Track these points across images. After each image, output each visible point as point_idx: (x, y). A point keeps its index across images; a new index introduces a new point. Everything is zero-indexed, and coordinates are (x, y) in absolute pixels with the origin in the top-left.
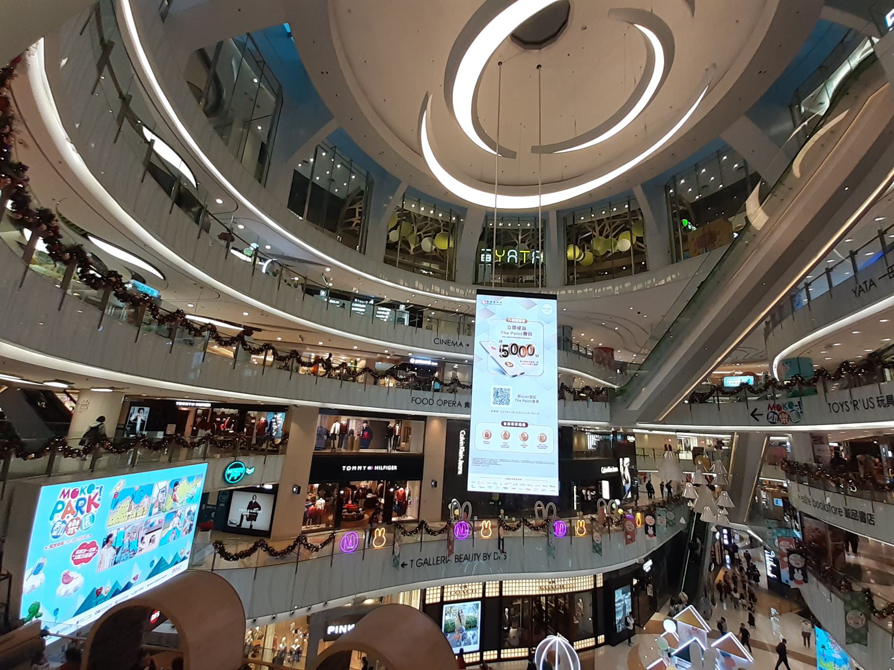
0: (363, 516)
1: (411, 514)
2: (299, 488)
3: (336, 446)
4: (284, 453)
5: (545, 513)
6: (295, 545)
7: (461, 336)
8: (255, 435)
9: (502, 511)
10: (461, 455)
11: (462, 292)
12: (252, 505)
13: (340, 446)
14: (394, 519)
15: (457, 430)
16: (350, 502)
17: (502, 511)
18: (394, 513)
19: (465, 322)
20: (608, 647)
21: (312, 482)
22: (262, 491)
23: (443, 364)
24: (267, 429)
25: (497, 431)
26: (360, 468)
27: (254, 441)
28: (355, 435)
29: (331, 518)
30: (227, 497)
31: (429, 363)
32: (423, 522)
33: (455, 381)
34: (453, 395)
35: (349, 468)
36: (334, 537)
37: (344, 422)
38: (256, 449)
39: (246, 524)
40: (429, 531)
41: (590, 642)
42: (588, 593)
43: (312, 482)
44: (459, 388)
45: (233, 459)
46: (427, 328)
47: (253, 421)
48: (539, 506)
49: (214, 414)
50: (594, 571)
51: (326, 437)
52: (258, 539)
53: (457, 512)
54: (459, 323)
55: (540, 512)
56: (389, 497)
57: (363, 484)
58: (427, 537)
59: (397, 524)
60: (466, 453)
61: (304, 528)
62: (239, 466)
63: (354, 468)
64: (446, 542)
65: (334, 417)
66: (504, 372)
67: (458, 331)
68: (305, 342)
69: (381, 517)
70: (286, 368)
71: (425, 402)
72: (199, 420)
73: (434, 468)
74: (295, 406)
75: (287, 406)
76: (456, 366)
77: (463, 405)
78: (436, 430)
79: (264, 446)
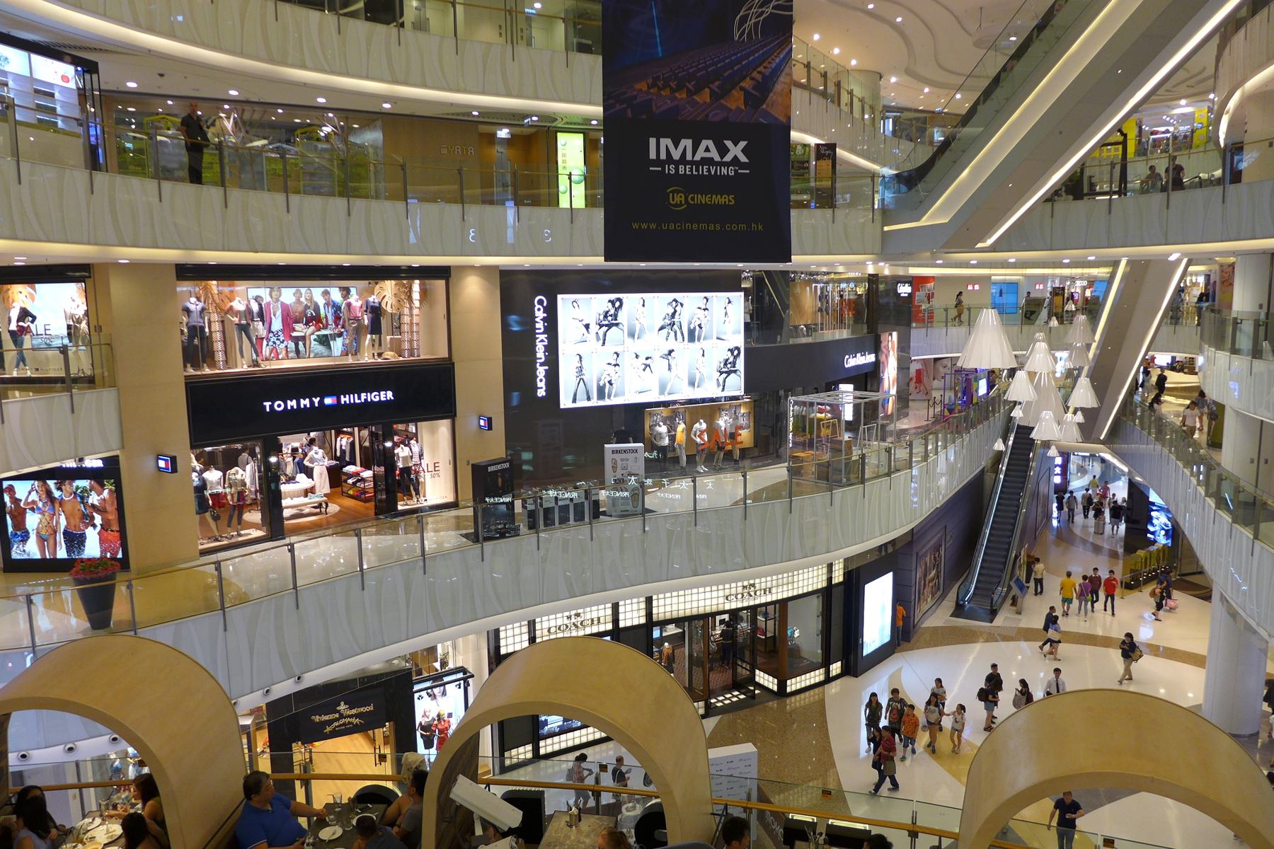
10: (540, 354)
20: (848, 681)
26: (305, 402)
35: (279, 406)
41: (817, 676)
42: (814, 597)
50: (828, 557)
63: (292, 404)
73: (480, 385)
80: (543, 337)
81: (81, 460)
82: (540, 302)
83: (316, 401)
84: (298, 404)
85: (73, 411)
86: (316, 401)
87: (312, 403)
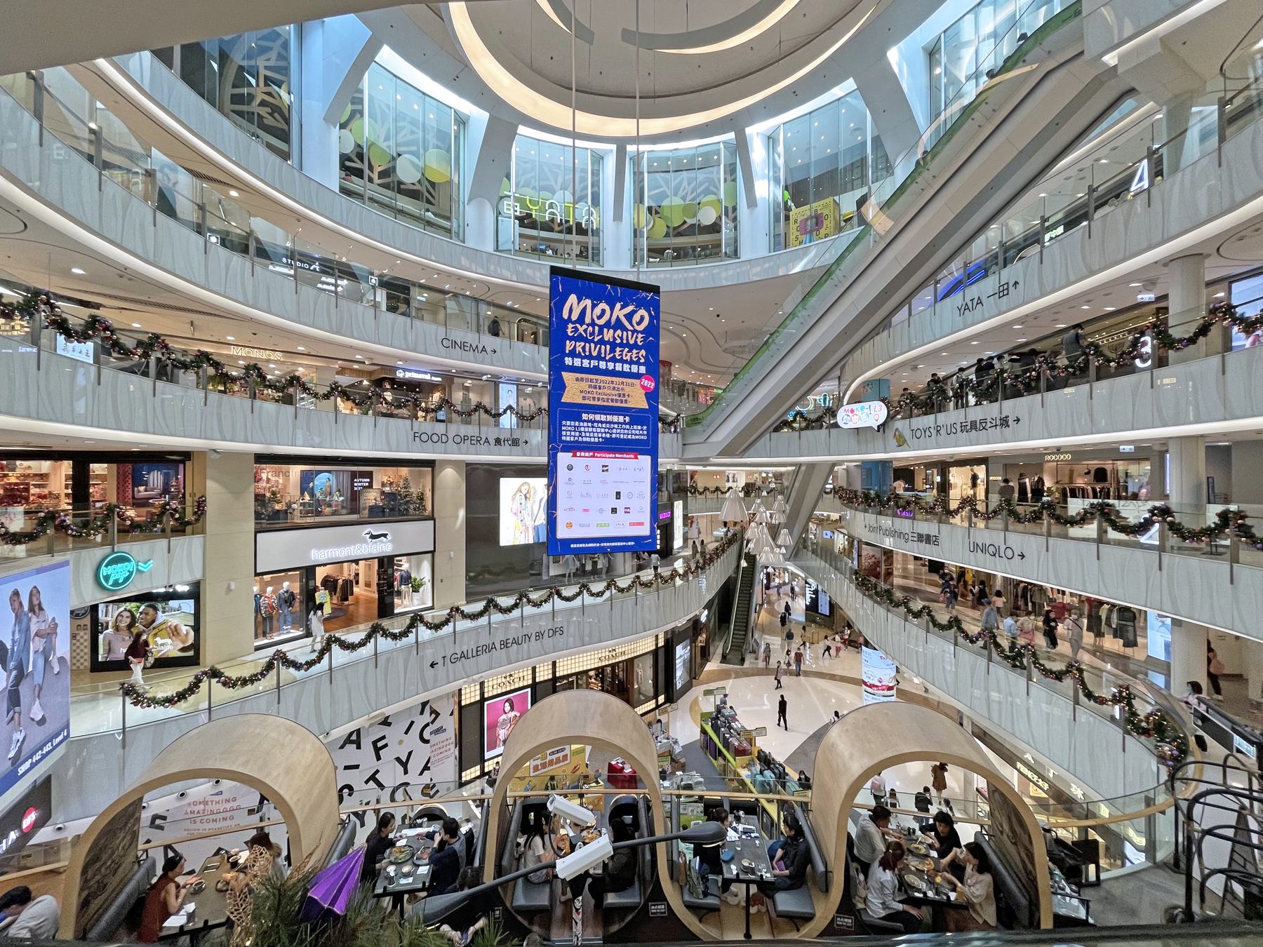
41: (652, 705)
50: (654, 632)
71: (435, 438)
77: (492, 442)
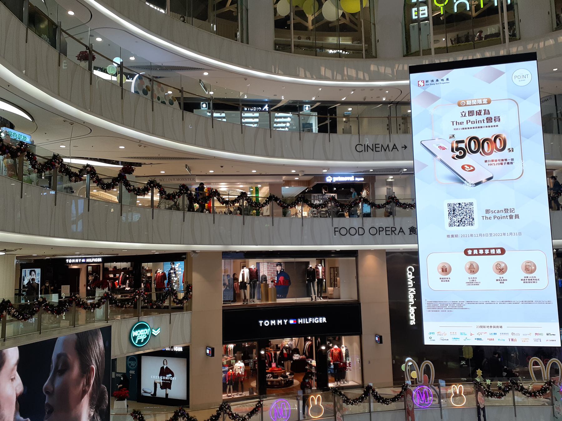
0: (291, 383)
1: (352, 378)
2: (213, 350)
3: (248, 297)
4: (189, 309)
5: (546, 374)
6: (219, 414)
7: (394, 136)
8: (153, 290)
9: (479, 372)
10: (411, 299)
11: (389, 71)
12: (164, 372)
13: (252, 296)
14: (331, 385)
15: (401, 268)
16: (274, 365)
17: (479, 372)
18: (330, 378)
19: (396, 115)
21: (226, 341)
22: (172, 354)
23: (371, 179)
24: (166, 282)
25: (459, 263)
26: (280, 322)
27: (154, 298)
28: (269, 282)
29: (254, 384)
30: (136, 363)
31: (352, 179)
32: (369, 388)
33: (392, 200)
34: (390, 219)
35: (267, 323)
36: (262, 405)
37: (253, 267)
38: (159, 307)
39: (161, 393)
40: (379, 399)
43: (226, 341)
44: (397, 209)
45: (135, 320)
46: (344, 132)
47: (149, 275)
48: (536, 363)
49: (106, 270)
51: (235, 288)
52: (177, 408)
53: (414, 374)
54: (389, 118)
55: (538, 374)
56: (322, 357)
57: (287, 342)
58: (375, 406)
59: (336, 391)
60: (418, 296)
61: (225, 396)
62: (142, 327)
63: (273, 322)
64: (403, 413)
65: (239, 261)
66: (461, 180)
67: (389, 128)
68: (192, 173)
69: (314, 383)
70: (176, 207)
71: (353, 231)
72: (91, 278)
73: (376, 317)
74: (194, 252)
75: (185, 254)
76: (390, 178)
77: (407, 231)
78: (373, 270)
79: (166, 303)
80: (413, 290)
81: (172, 347)
82: (410, 270)
83: (286, 321)
84: (276, 322)
85: (170, 323)
86: (286, 321)
87: (283, 322)
